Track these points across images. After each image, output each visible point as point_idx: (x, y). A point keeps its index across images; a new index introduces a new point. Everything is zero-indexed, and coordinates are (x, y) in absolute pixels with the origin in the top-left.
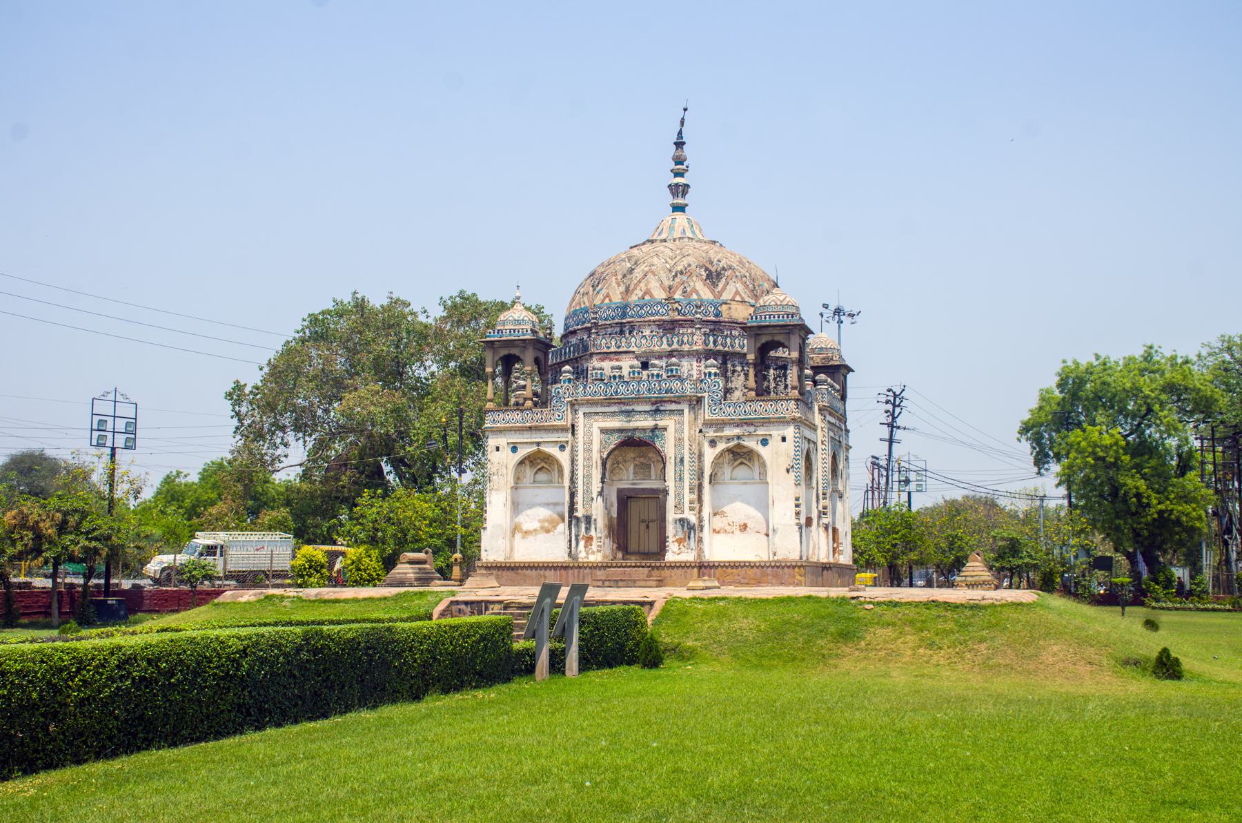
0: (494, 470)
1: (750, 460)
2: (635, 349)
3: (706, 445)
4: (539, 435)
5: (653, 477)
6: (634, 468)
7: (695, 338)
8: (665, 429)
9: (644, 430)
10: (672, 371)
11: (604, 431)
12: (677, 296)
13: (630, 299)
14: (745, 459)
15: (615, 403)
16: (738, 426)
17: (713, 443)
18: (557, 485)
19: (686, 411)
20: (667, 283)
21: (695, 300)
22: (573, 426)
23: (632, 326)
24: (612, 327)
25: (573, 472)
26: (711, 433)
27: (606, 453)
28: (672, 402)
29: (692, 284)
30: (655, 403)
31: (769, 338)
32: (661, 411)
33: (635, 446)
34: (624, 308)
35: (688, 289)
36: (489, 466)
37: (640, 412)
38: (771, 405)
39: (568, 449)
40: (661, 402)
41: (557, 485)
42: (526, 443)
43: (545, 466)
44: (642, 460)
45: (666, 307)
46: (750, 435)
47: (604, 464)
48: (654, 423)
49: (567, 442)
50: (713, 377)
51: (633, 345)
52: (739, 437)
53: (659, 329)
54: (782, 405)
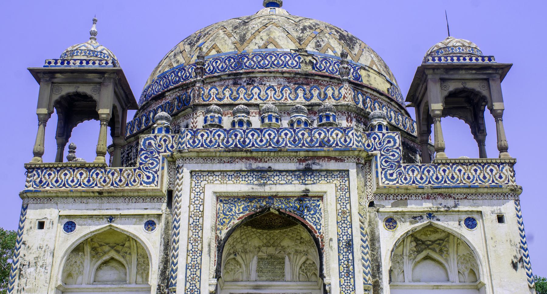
0: (30, 258)
1: (441, 251)
2: (259, 101)
3: (381, 226)
4: (114, 206)
5: (288, 277)
6: (259, 262)
7: (343, 91)
8: (321, 198)
9: (287, 198)
10: (328, 117)
11: (221, 198)
12: (310, 48)
13: (246, 49)
14: (434, 250)
15: (242, 158)
16: (428, 198)
17: (391, 222)
18: (133, 286)
19: (353, 172)
20: (295, 34)
21: (332, 57)
22: (170, 193)
23: (250, 78)
24: (221, 80)
25: (166, 262)
26: (388, 208)
27: (225, 232)
28: (330, 158)
29: (325, 39)
30: (305, 159)
31: (458, 85)
32: (313, 171)
33: (263, 228)
34: (240, 58)
35: (323, 44)
36: (22, 251)
37: (280, 171)
38: (476, 170)
39: (160, 227)
40: (313, 158)
41: (133, 286)
42: (91, 217)
43: (117, 257)
44: (271, 250)
45: (296, 59)
46: (448, 211)
47: (220, 248)
48: (303, 188)
49: (159, 216)
50: (384, 131)
51: (256, 96)
52: (430, 215)
53: (289, 83)
54: (491, 171)
